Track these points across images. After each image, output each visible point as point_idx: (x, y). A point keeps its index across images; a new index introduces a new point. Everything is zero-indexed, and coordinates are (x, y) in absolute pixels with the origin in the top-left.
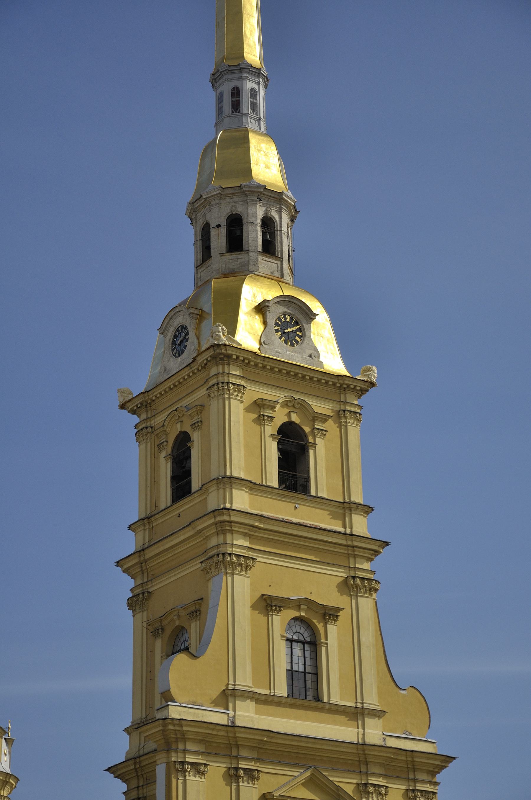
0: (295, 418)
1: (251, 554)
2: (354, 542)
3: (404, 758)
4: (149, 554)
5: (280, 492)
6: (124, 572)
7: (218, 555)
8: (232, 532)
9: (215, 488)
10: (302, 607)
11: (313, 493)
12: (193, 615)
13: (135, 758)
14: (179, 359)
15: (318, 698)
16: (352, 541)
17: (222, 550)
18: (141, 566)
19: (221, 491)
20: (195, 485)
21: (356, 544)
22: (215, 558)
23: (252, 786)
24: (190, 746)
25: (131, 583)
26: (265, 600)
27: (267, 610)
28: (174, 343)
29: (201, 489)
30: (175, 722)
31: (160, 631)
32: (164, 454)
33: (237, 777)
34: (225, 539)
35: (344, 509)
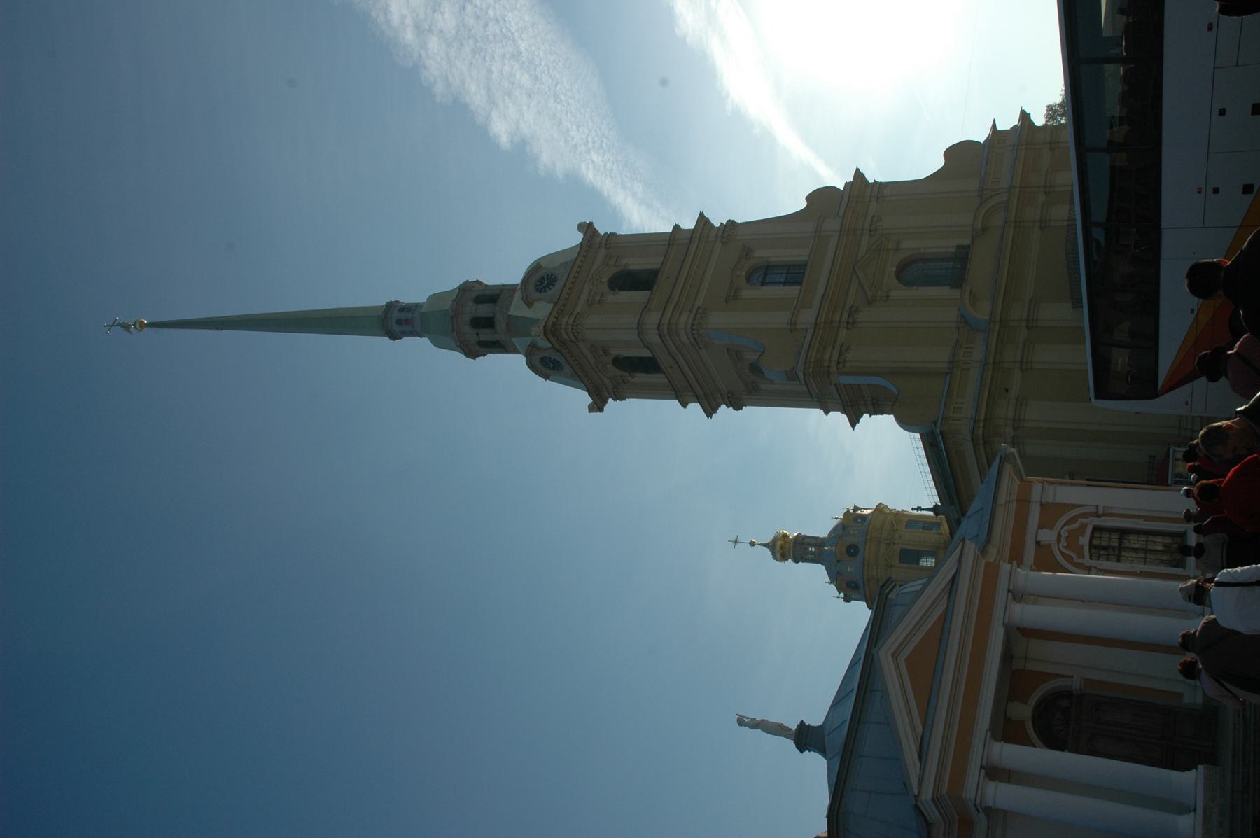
0: (605, 280)
4: (700, 392)
5: (654, 290)
6: (716, 412)
7: (693, 334)
11: (658, 267)
13: (844, 407)
14: (564, 365)
15: (804, 266)
20: (646, 353)
22: (695, 336)
25: (723, 406)
28: (553, 369)
29: (648, 348)
31: (754, 385)
32: (630, 379)
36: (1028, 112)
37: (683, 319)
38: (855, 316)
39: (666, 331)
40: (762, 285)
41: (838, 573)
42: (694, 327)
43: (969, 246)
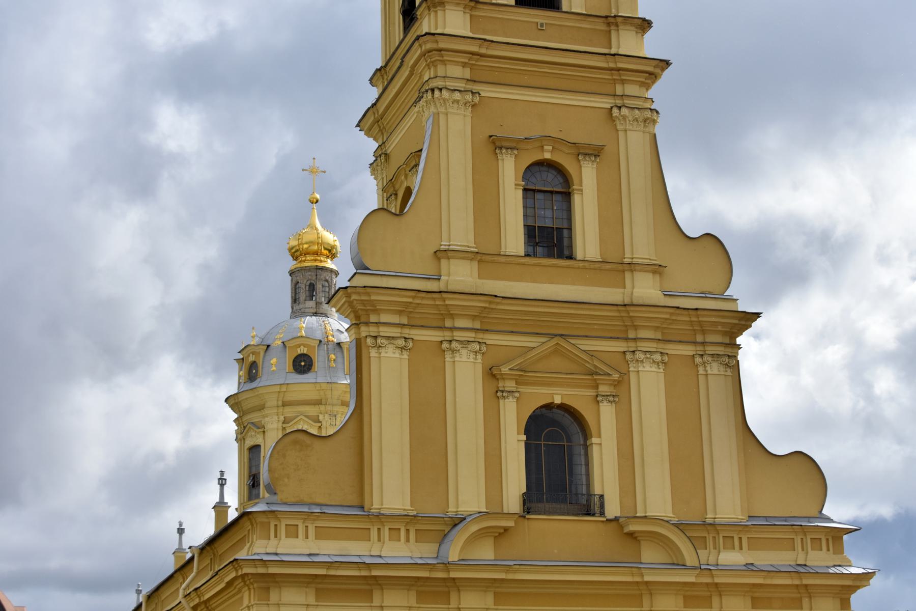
1: (470, 86)
2: (618, 63)
3: (687, 319)
4: (382, 107)
8: (444, 62)
9: (426, 12)
10: (546, 147)
12: (413, 172)
15: (571, 257)
16: (616, 63)
17: (433, 84)
18: (378, 125)
19: (432, 14)
21: (620, 65)
23: (467, 360)
24: (384, 318)
26: (494, 143)
27: (497, 154)
30: (358, 290)
33: (453, 351)
34: (436, 71)
35: (609, 24)
36: (872, 581)
37: (456, 71)
38: (464, 352)
39: (429, 46)
40: (525, 190)
41: (268, 346)
42: (437, 92)
43: (602, 514)
